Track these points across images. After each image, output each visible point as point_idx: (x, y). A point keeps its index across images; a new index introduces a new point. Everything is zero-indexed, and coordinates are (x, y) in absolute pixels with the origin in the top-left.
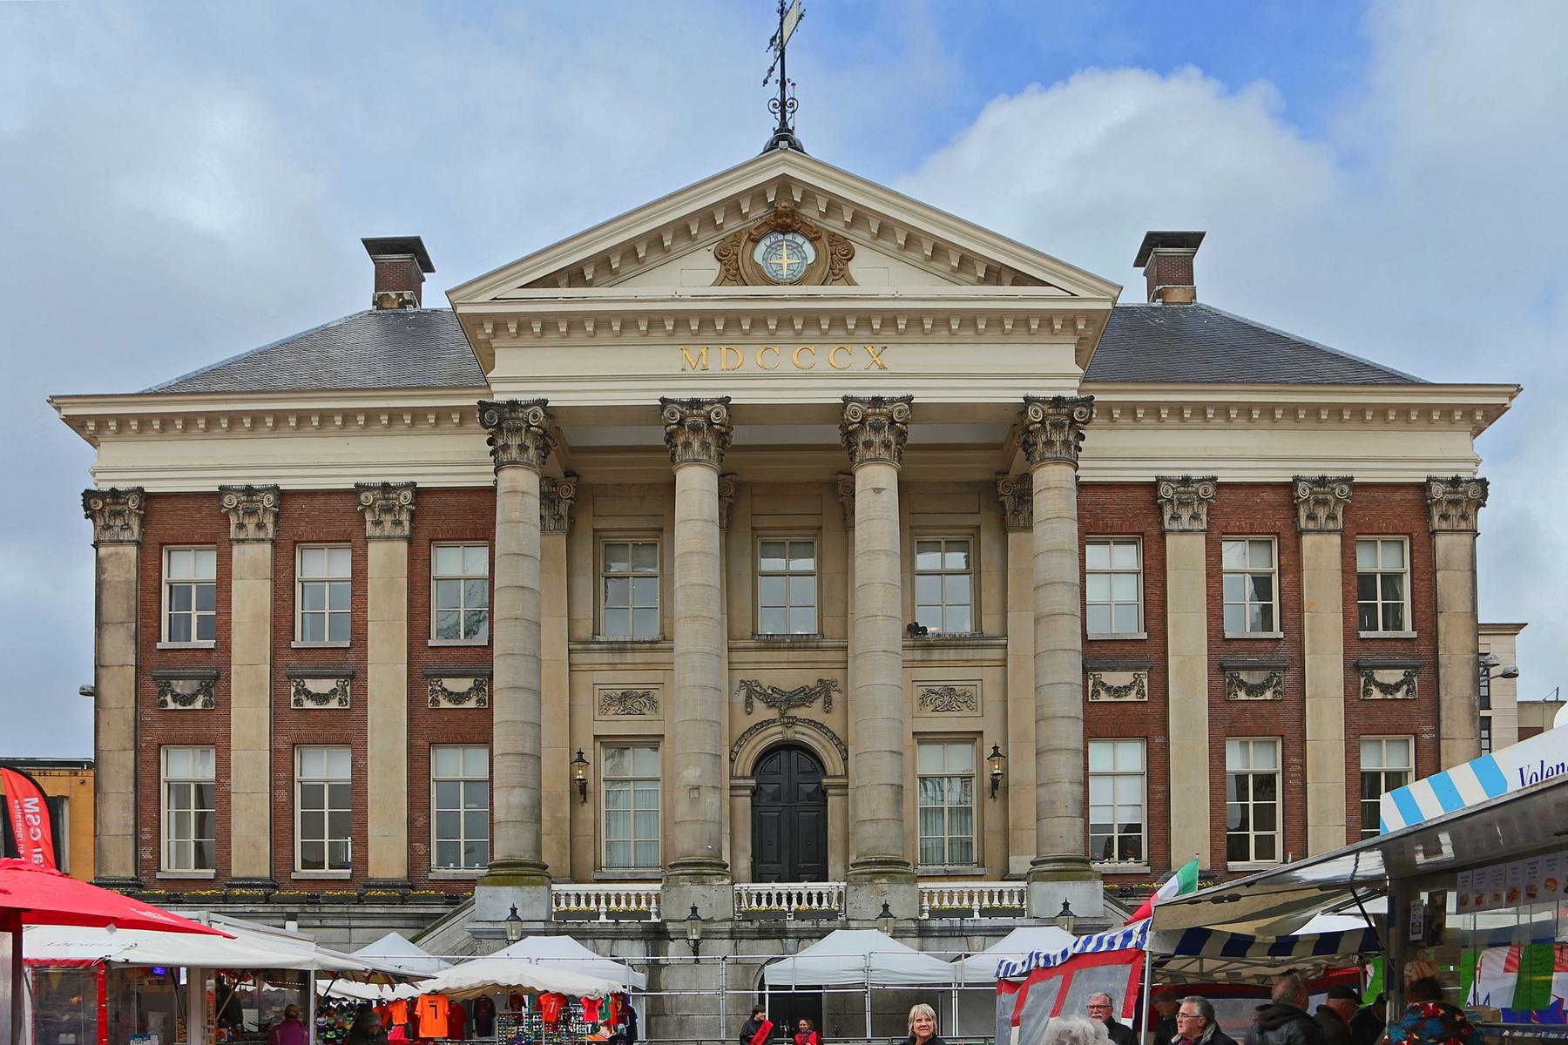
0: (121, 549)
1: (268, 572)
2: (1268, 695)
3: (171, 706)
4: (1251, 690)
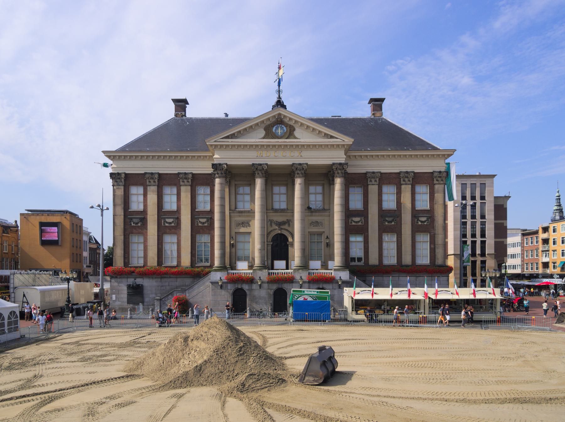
2: (393, 223)
3: (133, 225)
4: (389, 222)
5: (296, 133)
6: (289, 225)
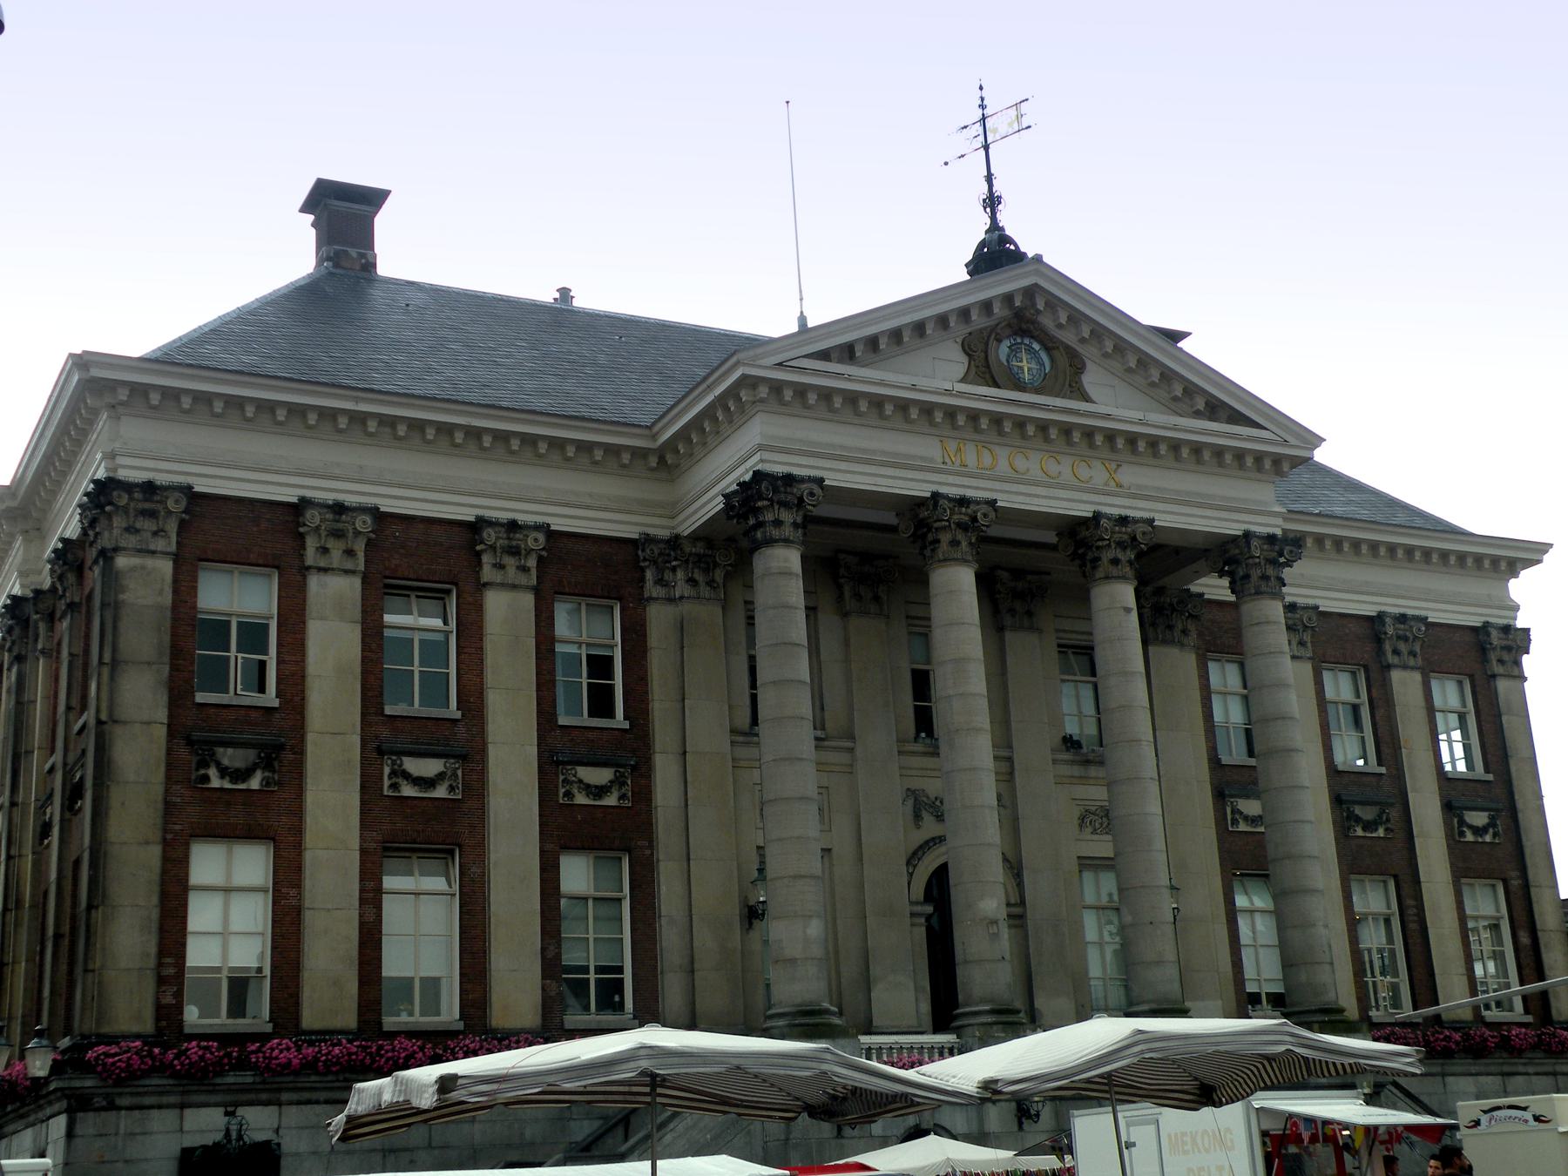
0: (150, 562)
1: (358, 615)
2: (1381, 832)
3: (216, 782)
4: (1367, 826)
5: (1092, 379)
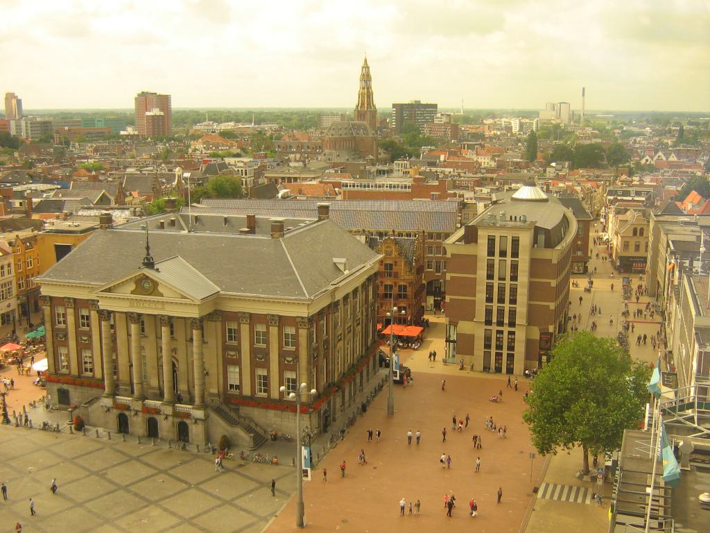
6: (176, 353)
